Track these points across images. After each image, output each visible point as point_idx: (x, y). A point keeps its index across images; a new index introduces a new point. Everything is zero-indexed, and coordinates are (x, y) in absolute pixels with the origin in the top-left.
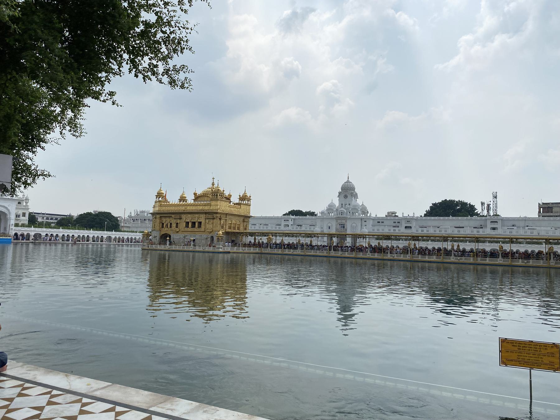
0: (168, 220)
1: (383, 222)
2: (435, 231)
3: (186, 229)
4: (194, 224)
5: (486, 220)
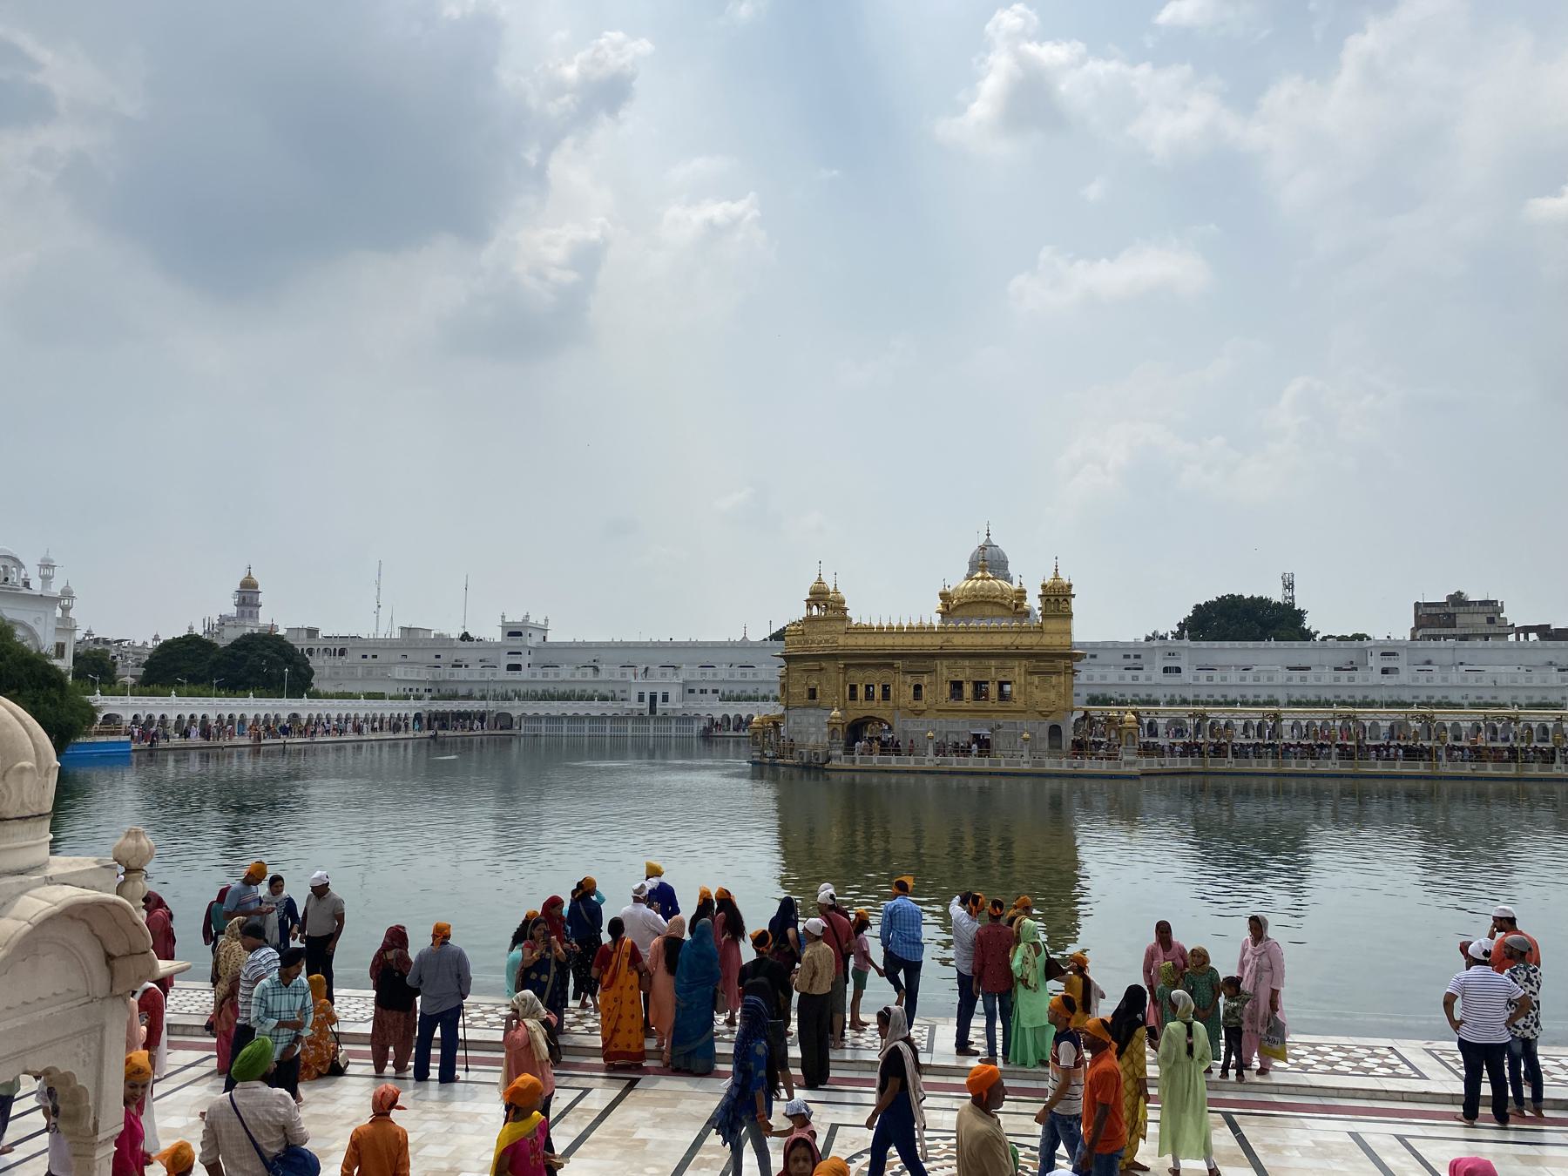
0: (877, 678)
1: (1094, 656)
2: (1243, 679)
3: (953, 704)
4: (979, 690)
5: (1365, 650)
